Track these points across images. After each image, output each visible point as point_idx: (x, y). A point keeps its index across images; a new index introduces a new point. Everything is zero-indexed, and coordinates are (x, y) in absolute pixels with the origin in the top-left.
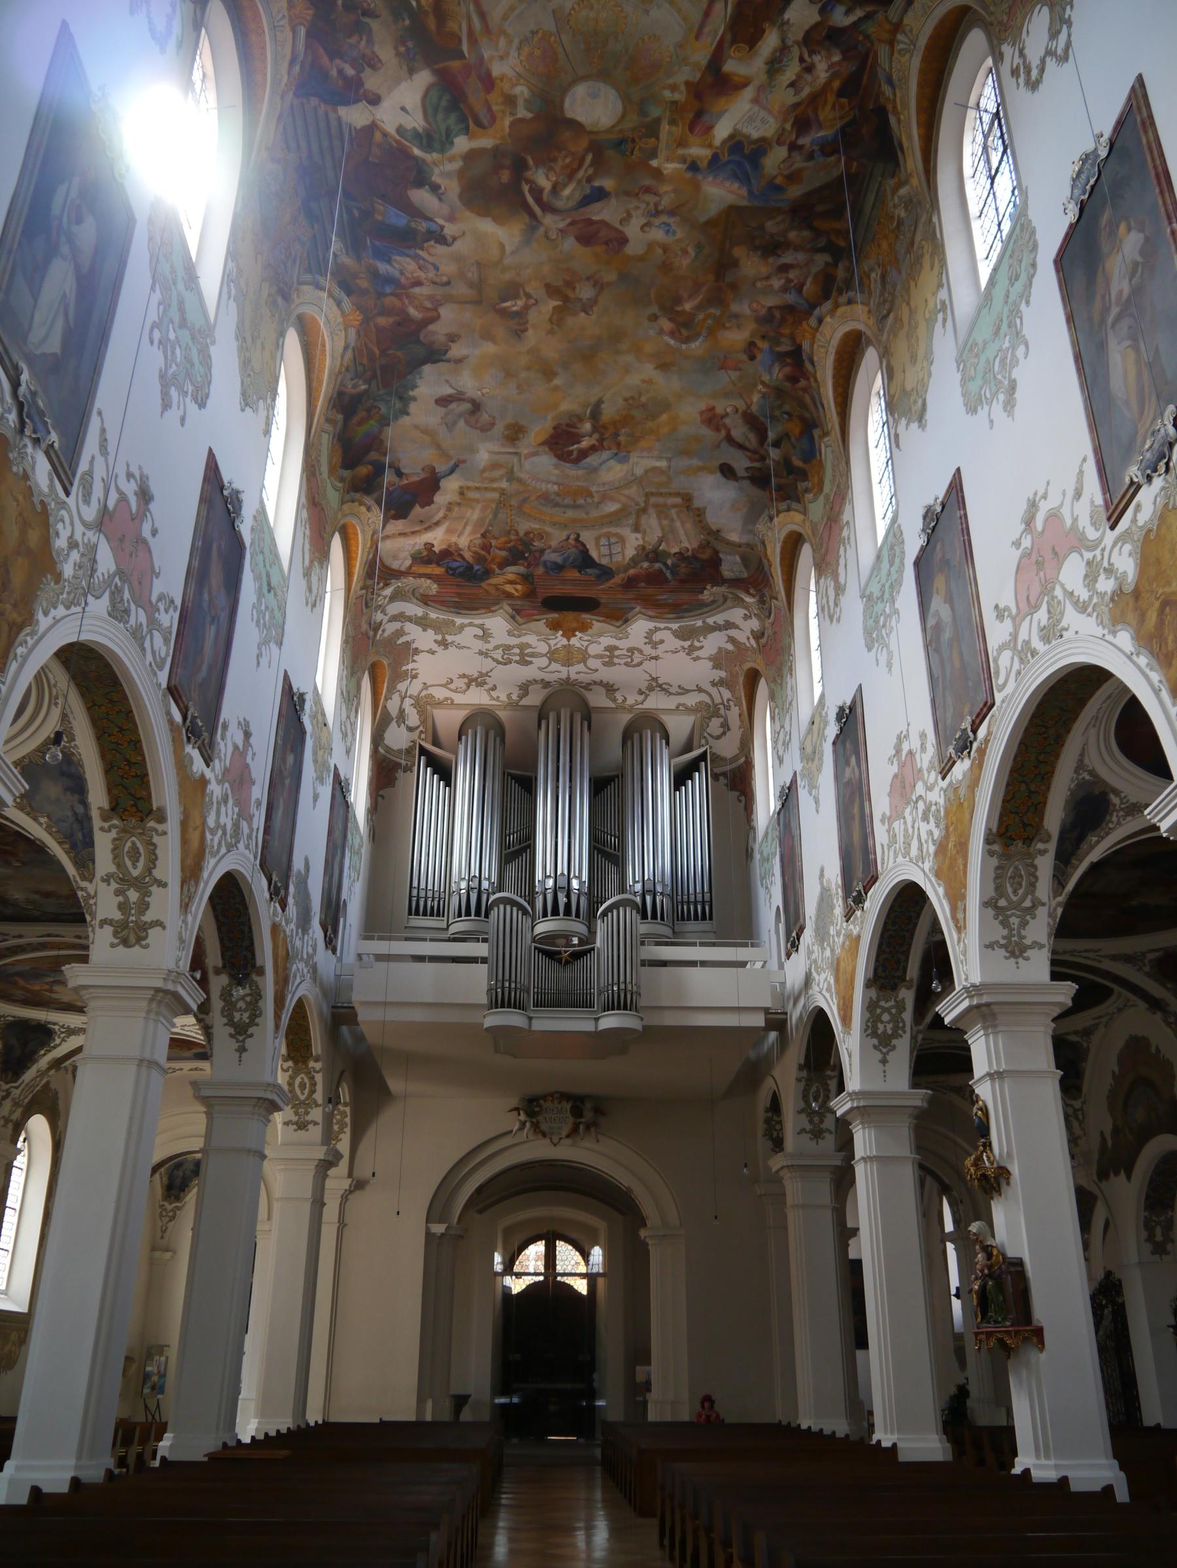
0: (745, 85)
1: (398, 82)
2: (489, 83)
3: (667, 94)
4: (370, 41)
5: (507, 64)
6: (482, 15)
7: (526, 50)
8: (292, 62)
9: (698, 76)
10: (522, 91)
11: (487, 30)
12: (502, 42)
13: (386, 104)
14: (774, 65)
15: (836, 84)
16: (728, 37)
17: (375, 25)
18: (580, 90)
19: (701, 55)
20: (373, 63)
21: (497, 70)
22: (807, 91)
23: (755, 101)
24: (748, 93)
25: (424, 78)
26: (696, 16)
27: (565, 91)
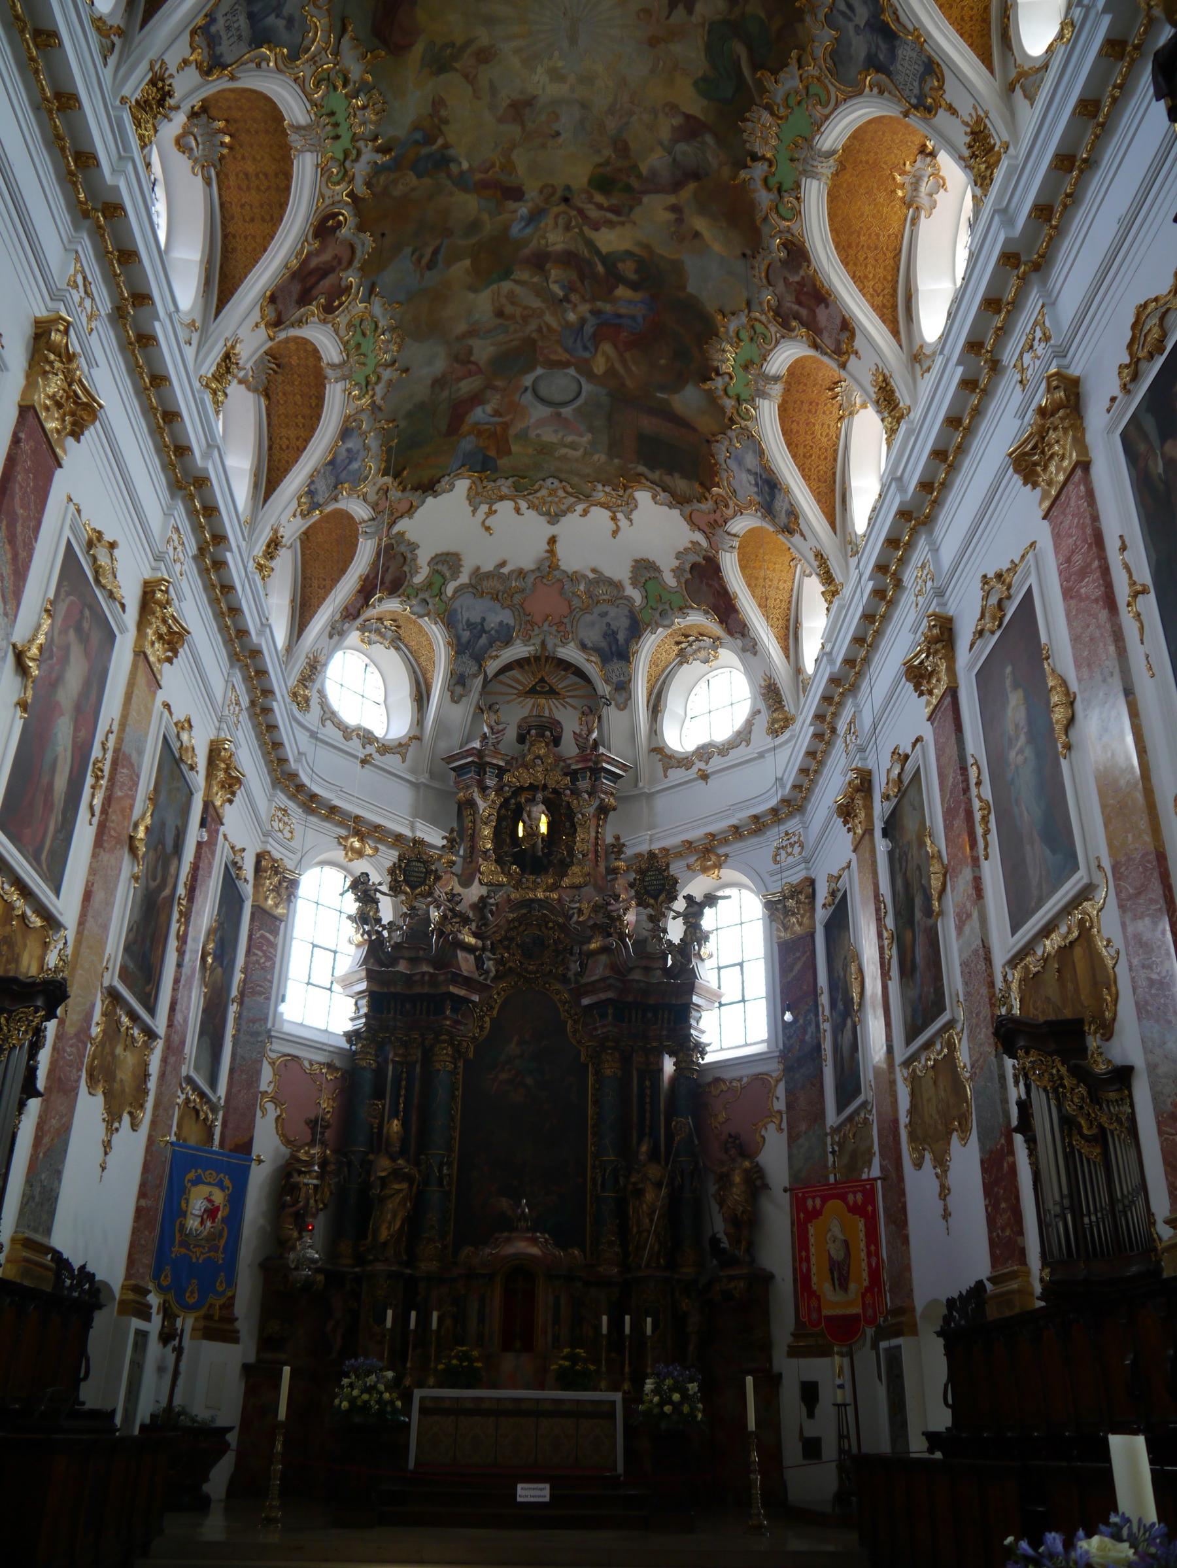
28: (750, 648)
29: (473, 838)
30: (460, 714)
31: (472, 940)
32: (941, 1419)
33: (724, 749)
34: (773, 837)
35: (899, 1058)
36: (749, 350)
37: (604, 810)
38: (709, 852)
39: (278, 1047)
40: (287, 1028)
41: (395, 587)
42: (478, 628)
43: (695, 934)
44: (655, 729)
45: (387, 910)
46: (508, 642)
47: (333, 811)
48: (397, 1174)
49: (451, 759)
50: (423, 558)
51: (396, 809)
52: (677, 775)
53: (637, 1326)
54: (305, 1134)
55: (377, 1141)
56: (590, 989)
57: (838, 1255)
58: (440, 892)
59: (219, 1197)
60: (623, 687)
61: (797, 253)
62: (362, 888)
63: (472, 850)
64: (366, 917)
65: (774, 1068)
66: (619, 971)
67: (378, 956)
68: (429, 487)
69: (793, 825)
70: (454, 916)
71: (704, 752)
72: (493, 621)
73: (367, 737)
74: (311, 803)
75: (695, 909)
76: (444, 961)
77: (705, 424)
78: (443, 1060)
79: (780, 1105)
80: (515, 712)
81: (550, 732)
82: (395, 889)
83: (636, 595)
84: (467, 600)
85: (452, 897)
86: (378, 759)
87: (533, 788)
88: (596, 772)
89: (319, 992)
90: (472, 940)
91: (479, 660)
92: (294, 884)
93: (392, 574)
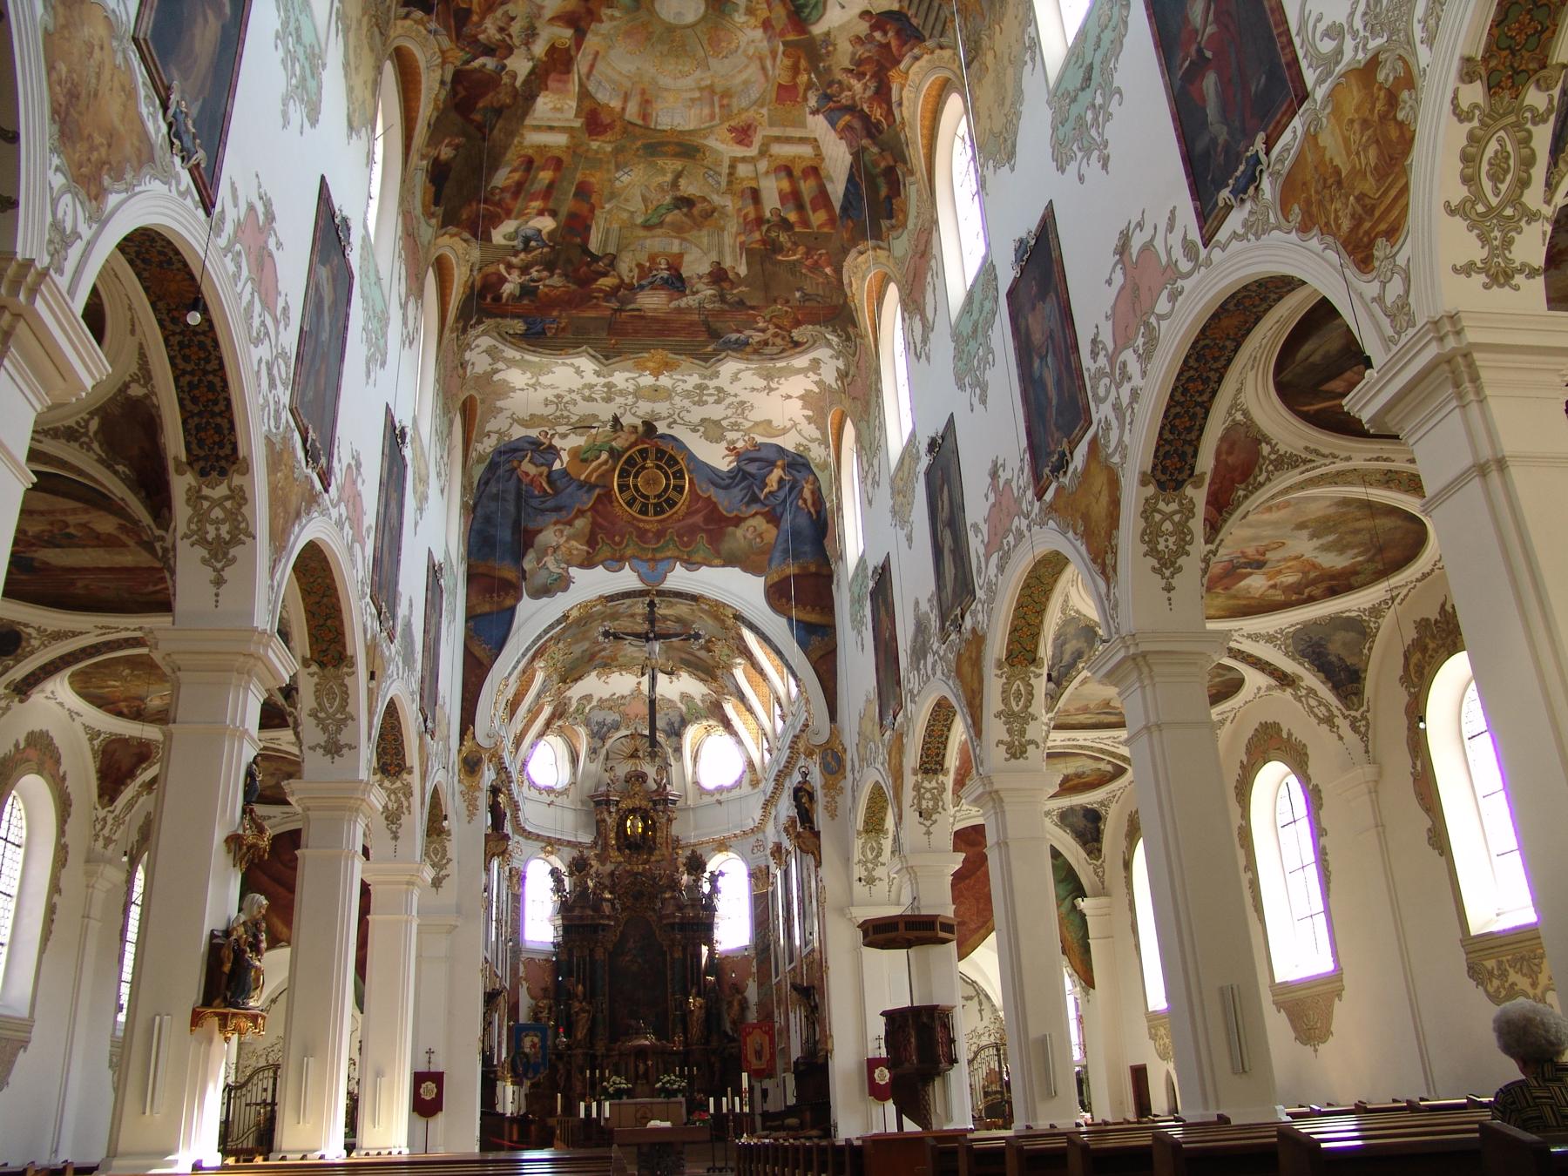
0: (552, 20)
1: (842, 27)
2: (767, 25)
3: (617, 14)
4: (854, 54)
5: (748, 35)
6: (763, 68)
7: (733, 46)
8: (917, 58)
9: (593, 26)
10: (740, 18)
11: (761, 59)
12: (751, 52)
13: (857, 11)
14: (531, 33)
15: (475, 18)
16: (573, 53)
17: (847, 64)
18: (690, 18)
19: (592, 42)
20: (858, 40)
21: (759, 33)
22: (499, 13)
23: (541, 7)
24: (548, 14)
25: (818, 30)
26: (600, 66)
27: (704, 18)
28: (740, 742)
29: (606, 838)
30: (596, 767)
31: (608, 896)
32: (791, 1101)
33: (729, 789)
34: (752, 840)
35: (788, 968)
36: (726, 651)
37: (670, 820)
38: (722, 846)
39: (524, 956)
40: (529, 945)
41: (560, 717)
42: (602, 724)
43: (715, 889)
44: (695, 773)
45: (567, 881)
46: (618, 729)
47: (538, 837)
48: (583, 1010)
49: (592, 797)
50: (574, 704)
51: (566, 823)
52: (707, 799)
53: (690, 1071)
54: (541, 993)
55: (571, 996)
56: (668, 916)
57: (758, 1047)
58: (592, 871)
59: (536, 1040)
60: (678, 750)
61: (741, 638)
62: (555, 873)
63: (606, 846)
64: (558, 888)
65: (752, 953)
66: (681, 908)
67: (565, 909)
68: (580, 678)
69: (760, 836)
70: (600, 885)
71: (720, 789)
72: (609, 721)
73: (550, 790)
74: (528, 835)
75: (714, 879)
76: (597, 908)
77: (710, 662)
78: (600, 954)
79: (754, 970)
80: (623, 769)
81: (641, 777)
82: (571, 874)
83: (684, 708)
84: (596, 712)
85: (598, 875)
86: (558, 801)
87: (633, 811)
88: (666, 801)
89: (541, 927)
90: (608, 896)
91: (603, 739)
92: (524, 878)
93: (559, 713)
